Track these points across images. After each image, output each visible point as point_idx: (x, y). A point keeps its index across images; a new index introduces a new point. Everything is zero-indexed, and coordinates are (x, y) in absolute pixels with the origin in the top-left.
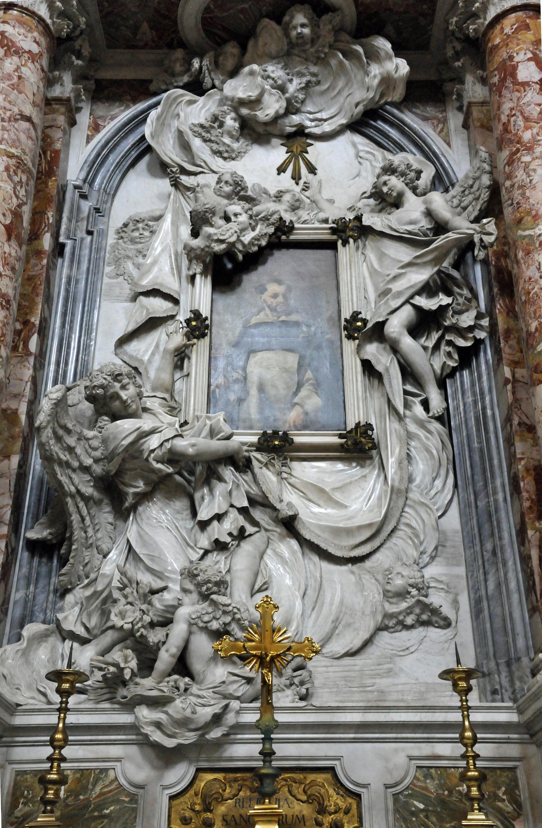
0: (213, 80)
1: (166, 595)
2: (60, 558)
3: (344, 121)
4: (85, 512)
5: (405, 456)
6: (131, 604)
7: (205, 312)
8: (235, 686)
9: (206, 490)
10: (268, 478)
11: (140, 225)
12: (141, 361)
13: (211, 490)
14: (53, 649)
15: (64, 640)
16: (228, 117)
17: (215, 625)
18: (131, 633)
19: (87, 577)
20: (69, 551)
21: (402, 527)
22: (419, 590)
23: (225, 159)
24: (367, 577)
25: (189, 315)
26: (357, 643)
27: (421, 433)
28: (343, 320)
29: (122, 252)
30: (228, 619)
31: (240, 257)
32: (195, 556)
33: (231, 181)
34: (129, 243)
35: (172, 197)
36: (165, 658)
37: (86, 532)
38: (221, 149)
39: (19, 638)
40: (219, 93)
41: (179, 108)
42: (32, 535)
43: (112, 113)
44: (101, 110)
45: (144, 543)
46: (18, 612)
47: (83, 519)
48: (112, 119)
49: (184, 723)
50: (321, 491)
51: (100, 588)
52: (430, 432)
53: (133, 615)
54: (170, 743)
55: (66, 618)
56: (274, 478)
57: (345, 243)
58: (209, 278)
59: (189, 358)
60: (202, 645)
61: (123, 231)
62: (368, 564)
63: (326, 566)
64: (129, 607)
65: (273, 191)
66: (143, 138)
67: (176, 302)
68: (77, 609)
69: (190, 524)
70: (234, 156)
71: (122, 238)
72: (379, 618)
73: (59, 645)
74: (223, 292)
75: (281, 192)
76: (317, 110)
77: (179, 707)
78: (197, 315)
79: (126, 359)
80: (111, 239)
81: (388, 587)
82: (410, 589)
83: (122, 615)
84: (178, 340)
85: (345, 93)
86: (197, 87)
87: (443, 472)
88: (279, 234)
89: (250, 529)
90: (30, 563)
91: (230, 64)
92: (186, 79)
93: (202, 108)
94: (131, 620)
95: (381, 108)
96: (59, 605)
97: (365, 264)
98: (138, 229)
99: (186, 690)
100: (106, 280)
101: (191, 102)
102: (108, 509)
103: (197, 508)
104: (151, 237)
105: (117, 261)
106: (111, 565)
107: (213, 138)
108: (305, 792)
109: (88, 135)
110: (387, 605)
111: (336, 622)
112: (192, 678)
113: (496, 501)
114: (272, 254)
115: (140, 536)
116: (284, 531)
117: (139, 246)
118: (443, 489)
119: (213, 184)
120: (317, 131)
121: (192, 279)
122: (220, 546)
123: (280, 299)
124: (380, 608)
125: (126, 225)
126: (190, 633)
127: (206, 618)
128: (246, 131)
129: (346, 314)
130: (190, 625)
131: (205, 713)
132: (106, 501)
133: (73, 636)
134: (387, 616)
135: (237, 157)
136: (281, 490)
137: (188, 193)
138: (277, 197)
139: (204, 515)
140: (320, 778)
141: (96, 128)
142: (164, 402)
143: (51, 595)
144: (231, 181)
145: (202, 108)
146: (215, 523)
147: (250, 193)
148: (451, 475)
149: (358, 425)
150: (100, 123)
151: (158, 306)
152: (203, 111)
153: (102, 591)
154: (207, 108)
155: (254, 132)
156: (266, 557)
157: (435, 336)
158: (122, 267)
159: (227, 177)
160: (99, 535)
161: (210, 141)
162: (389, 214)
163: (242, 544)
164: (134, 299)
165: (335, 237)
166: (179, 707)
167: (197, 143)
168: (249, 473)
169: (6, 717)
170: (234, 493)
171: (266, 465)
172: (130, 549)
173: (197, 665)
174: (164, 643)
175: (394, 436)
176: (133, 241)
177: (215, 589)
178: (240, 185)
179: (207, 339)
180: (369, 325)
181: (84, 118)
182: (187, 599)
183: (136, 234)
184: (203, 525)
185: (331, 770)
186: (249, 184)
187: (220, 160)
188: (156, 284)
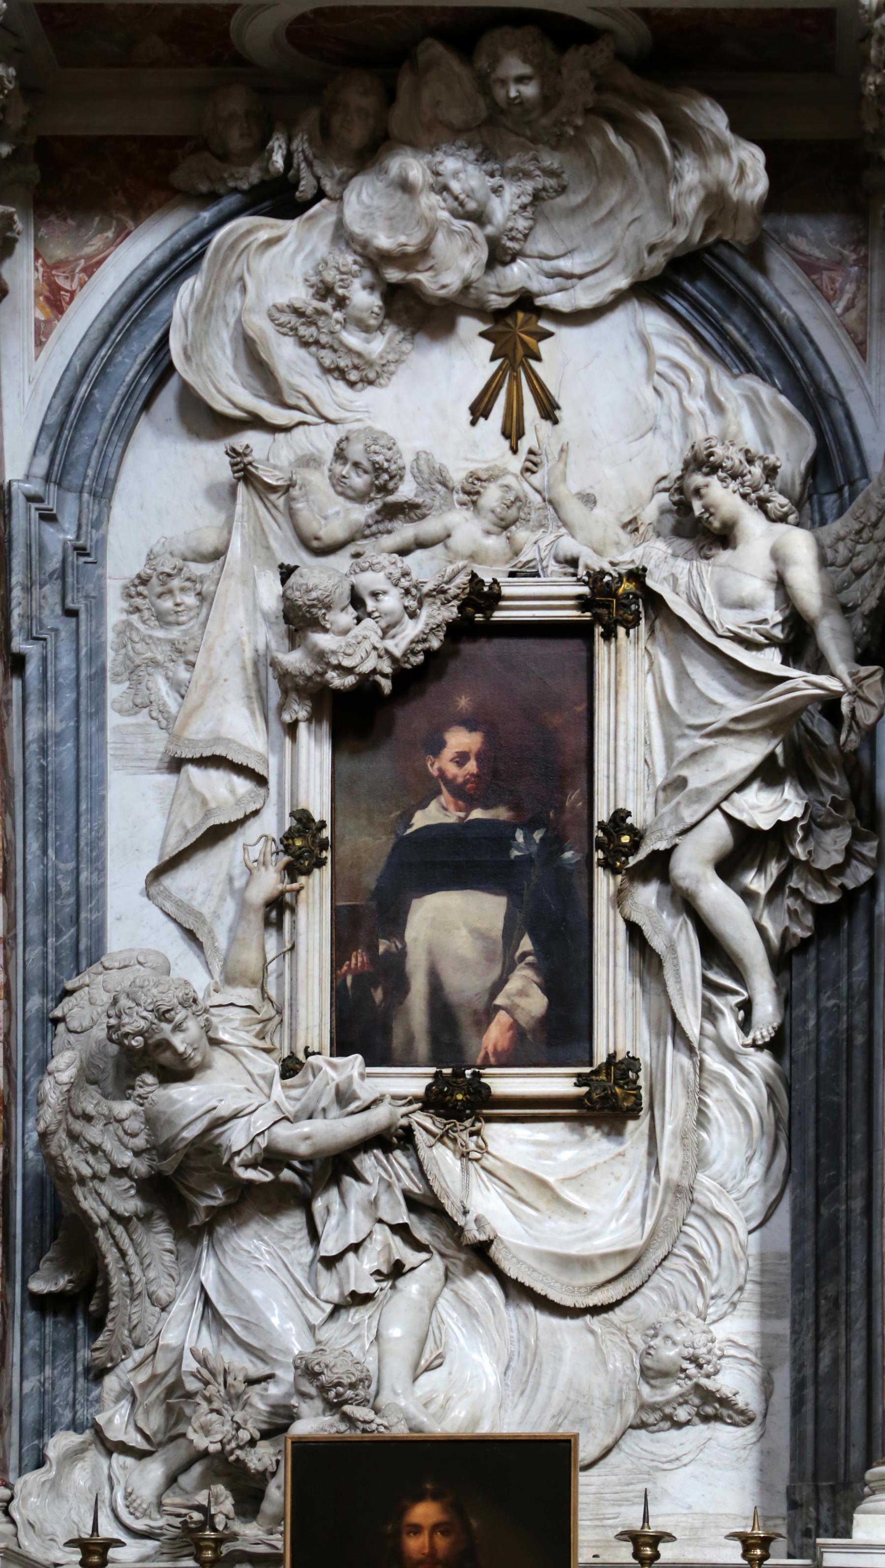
0: (318, 179)
1: (274, 1390)
2: (87, 1316)
3: (623, 283)
6: (219, 1412)
7: (320, 810)
9: (334, 1193)
10: (443, 1162)
11: (176, 583)
12: (199, 916)
14: (95, 1469)
15: (109, 1454)
18: (222, 1455)
19: (137, 1346)
20: (105, 1309)
23: (352, 384)
25: (288, 823)
27: (730, 1073)
28: (596, 824)
29: (139, 647)
33: (366, 464)
34: (154, 622)
37: (129, 1274)
38: (342, 364)
39: (40, 1462)
40: (334, 206)
42: (38, 1286)
43: (88, 250)
45: (232, 1298)
46: (31, 1413)
47: (123, 1254)
48: (90, 271)
50: (543, 1184)
51: (161, 1369)
53: (221, 1429)
55: (110, 1420)
57: (609, 635)
58: (325, 728)
59: (293, 911)
61: (139, 594)
63: (544, 1320)
64: (214, 1416)
65: (458, 476)
66: (164, 340)
67: (261, 781)
68: (125, 1404)
70: (372, 375)
71: (138, 610)
72: (630, 1410)
73: (104, 1462)
74: (355, 752)
75: (479, 479)
76: (562, 250)
79: (169, 907)
80: (115, 611)
81: (648, 1362)
82: (686, 1365)
83: (206, 1430)
84: (269, 882)
88: (470, 609)
90: (41, 1329)
91: (357, 135)
93: (296, 252)
94: (219, 1437)
95: (708, 249)
96: (95, 1394)
97: (650, 678)
98: (170, 592)
100: (113, 719)
102: (163, 1226)
103: (320, 1229)
104: (199, 607)
105: (133, 672)
107: (324, 339)
109: (37, 321)
110: (645, 1390)
113: (849, 1211)
114: (456, 654)
116: (475, 1260)
117: (175, 633)
120: (559, 301)
121: (291, 729)
124: (633, 1394)
125: (144, 581)
128: (399, 305)
129: (602, 813)
132: (158, 1213)
133: (124, 1449)
134: (644, 1407)
135: (378, 376)
137: (273, 497)
138: (468, 493)
141: (56, 301)
142: (251, 1015)
143: (81, 1381)
144: (366, 464)
145: (296, 252)
147: (406, 491)
149: (611, 1057)
150: (61, 282)
151: (223, 792)
152: (299, 259)
153: (166, 1374)
154: (308, 249)
155: (418, 313)
158: (143, 687)
160: (152, 1274)
161: (317, 343)
162: (707, 558)
164: (176, 765)
167: (287, 357)
168: (412, 1151)
172: (207, 1302)
175: (679, 1079)
176: (162, 619)
178: (386, 471)
179: (327, 869)
183: (167, 604)
186: (407, 460)
187: (340, 387)
188: (218, 740)
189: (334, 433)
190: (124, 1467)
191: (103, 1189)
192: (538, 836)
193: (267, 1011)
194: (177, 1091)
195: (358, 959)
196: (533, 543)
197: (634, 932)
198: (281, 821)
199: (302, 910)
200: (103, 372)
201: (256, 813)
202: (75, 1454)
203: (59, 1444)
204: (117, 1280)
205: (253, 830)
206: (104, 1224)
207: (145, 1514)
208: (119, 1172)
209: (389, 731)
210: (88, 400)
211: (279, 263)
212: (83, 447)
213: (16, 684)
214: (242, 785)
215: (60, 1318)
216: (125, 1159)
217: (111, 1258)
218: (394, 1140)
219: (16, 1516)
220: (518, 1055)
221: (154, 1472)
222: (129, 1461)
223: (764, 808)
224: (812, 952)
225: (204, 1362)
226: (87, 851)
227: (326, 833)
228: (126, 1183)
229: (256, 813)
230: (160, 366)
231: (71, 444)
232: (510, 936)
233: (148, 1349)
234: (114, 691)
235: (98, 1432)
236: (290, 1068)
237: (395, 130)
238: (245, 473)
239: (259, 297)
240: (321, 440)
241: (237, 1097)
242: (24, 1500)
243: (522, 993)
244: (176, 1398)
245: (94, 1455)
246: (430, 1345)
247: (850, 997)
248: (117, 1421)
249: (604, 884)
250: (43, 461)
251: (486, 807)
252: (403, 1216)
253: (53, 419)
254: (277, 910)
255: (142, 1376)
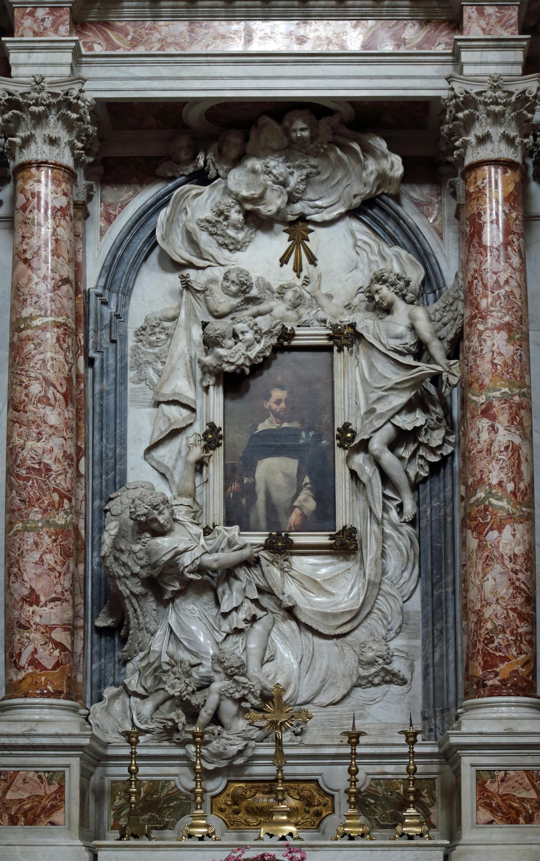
4: (137, 606)
5: (379, 556)
7: (219, 423)
8: (252, 732)
11: (157, 330)
12: (167, 468)
13: (230, 587)
16: (233, 210)
17: (237, 695)
20: (127, 634)
21: (375, 611)
22: (384, 660)
24: (347, 649)
26: (338, 697)
30: (246, 692)
31: (247, 371)
32: (220, 638)
35: (184, 296)
36: (204, 715)
37: (138, 619)
41: (186, 202)
44: (112, 194)
46: (96, 678)
49: (219, 755)
50: (315, 582)
51: (152, 660)
52: (401, 533)
54: (210, 767)
55: (130, 682)
56: (278, 573)
60: (229, 707)
62: (349, 638)
67: (193, 410)
68: (137, 675)
69: (214, 611)
73: (127, 700)
74: (233, 399)
77: (215, 745)
78: (212, 426)
85: (344, 184)
86: (202, 178)
87: (410, 566)
89: (260, 613)
92: (191, 169)
99: (219, 734)
100: (130, 385)
101: (197, 195)
105: (138, 366)
106: (159, 644)
108: (298, 794)
111: (324, 681)
112: (223, 726)
115: (179, 623)
118: (409, 578)
119: (221, 278)
122: (238, 631)
123: (283, 405)
125: (144, 329)
126: (221, 700)
127: (231, 691)
129: (339, 424)
130: (220, 695)
131: (233, 750)
136: (283, 582)
139: (225, 608)
140: (308, 786)
146: (234, 613)
148: (417, 567)
156: (273, 635)
157: (412, 447)
159: (233, 276)
163: (255, 625)
164: (157, 404)
165: (331, 343)
166: (215, 745)
167: (204, 238)
169: (100, 749)
170: (248, 588)
171: (272, 562)
172: (172, 631)
173: (226, 720)
174: (203, 706)
177: (237, 671)
179: (221, 449)
180: (357, 441)
181: (96, 208)
182: (217, 677)
183: (153, 338)
184: (225, 615)
185: (317, 781)
189: (223, 270)
190: (136, 703)
191: (128, 582)
192: (311, 434)
193: (196, 508)
194: (159, 540)
195: (235, 486)
196: (306, 314)
197: (354, 474)
198: (202, 428)
199: (211, 465)
200: (128, 246)
201: (191, 424)
202: (115, 696)
203: (109, 691)
204: (133, 622)
205: (190, 432)
206: (128, 597)
207: (146, 723)
208: (135, 575)
209: (247, 390)
210: (122, 257)
211: (202, 203)
212: (119, 275)
213: (90, 370)
214: (185, 412)
215: (108, 638)
216: (137, 569)
217: (131, 612)
218: (251, 563)
219: (91, 721)
220: (305, 526)
221: (148, 707)
222: (138, 700)
223: (407, 422)
224: (428, 483)
225: (171, 657)
226: (120, 440)
227: (221, 433)
228: (136, 580)
229: (191, 424)
230: (152, 243)
231: (115, 274)
232: (300, 475)
233: (146, 651)
234: (131, 374)
235: (125, 687)
236: (207, 531)
237: (248, 150)
238: (187, 285)
239: (193, 215)
240: (218, 273)
241: (184, 544)
242: (94, 715)
243: (305, 500)
244: (158, 672)
245: (124, 697)
246: (268, 651)
247: (445, 501)
248: (133, 682)
249: (340, 454)
250: (103, 280)
251: (289, 421)
252: (255, 595)
253: (107, 264)
254: (200, 465)
255: (144, 664)
